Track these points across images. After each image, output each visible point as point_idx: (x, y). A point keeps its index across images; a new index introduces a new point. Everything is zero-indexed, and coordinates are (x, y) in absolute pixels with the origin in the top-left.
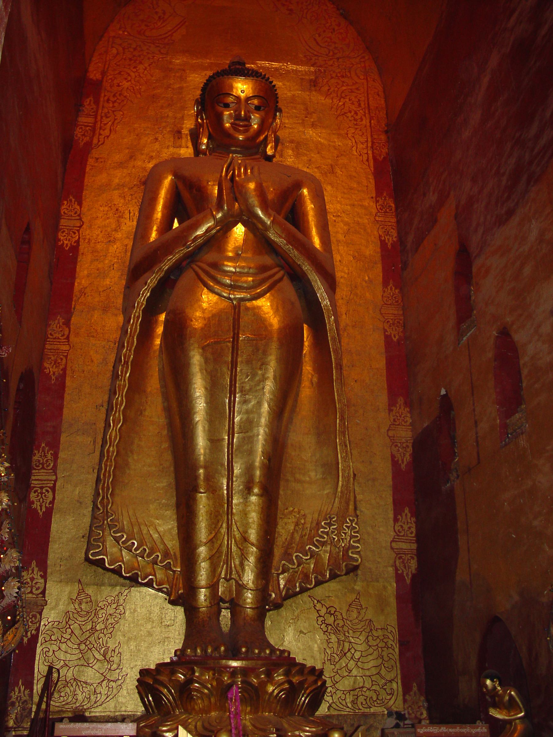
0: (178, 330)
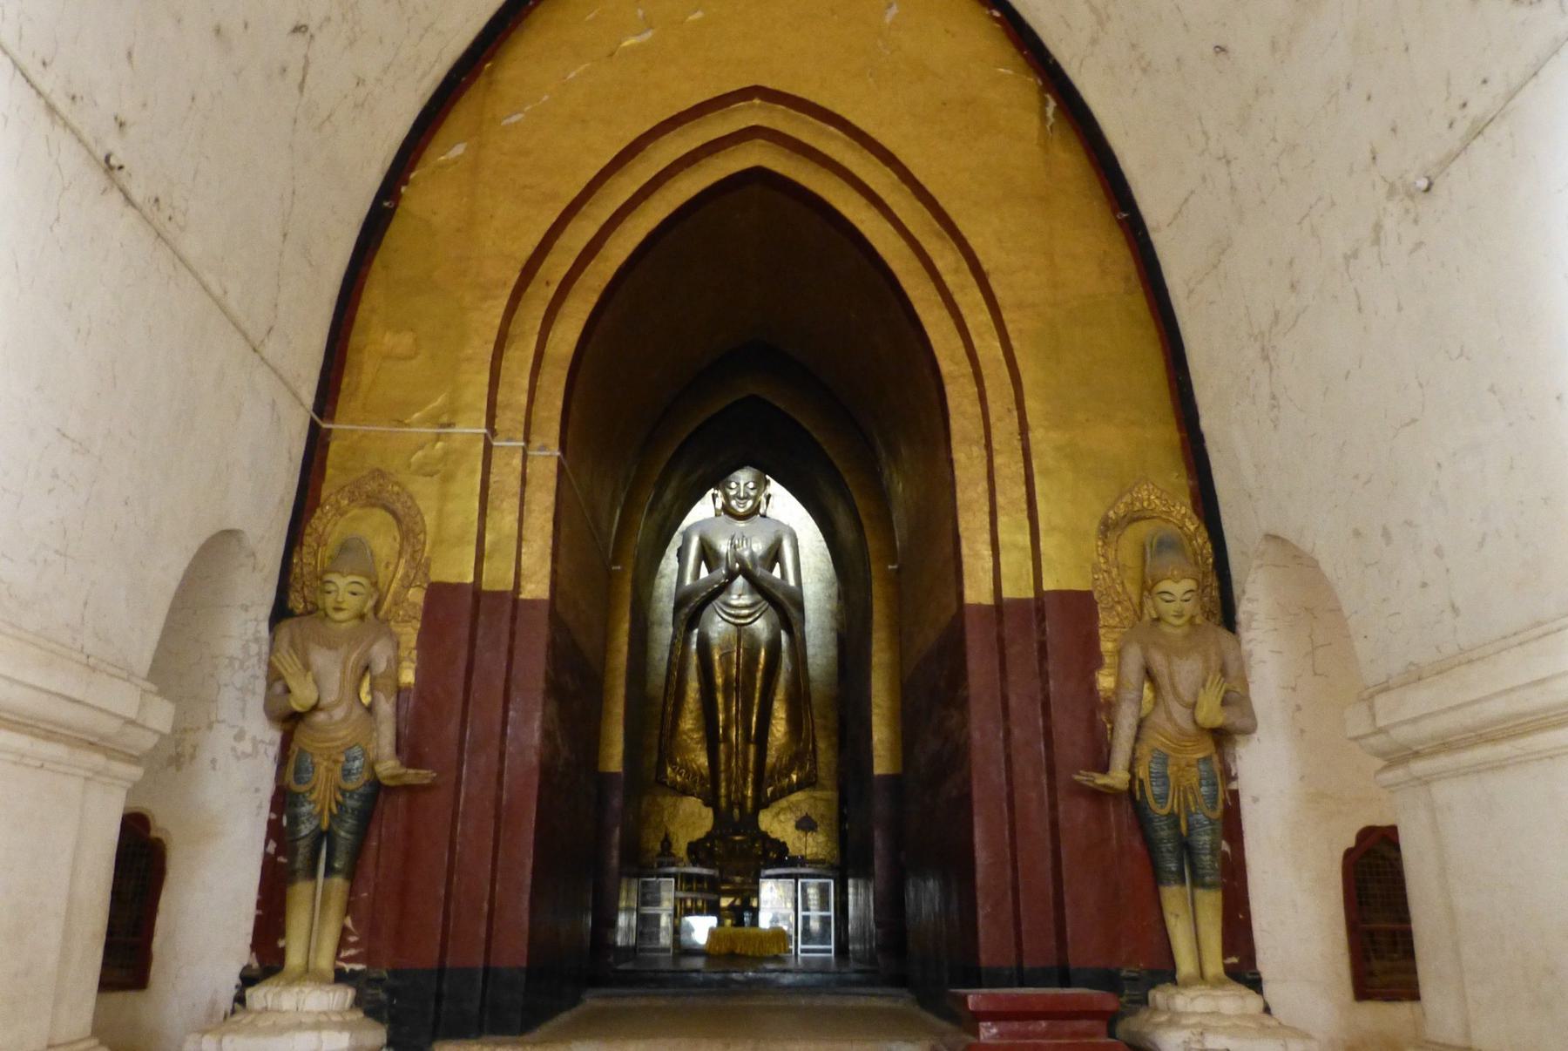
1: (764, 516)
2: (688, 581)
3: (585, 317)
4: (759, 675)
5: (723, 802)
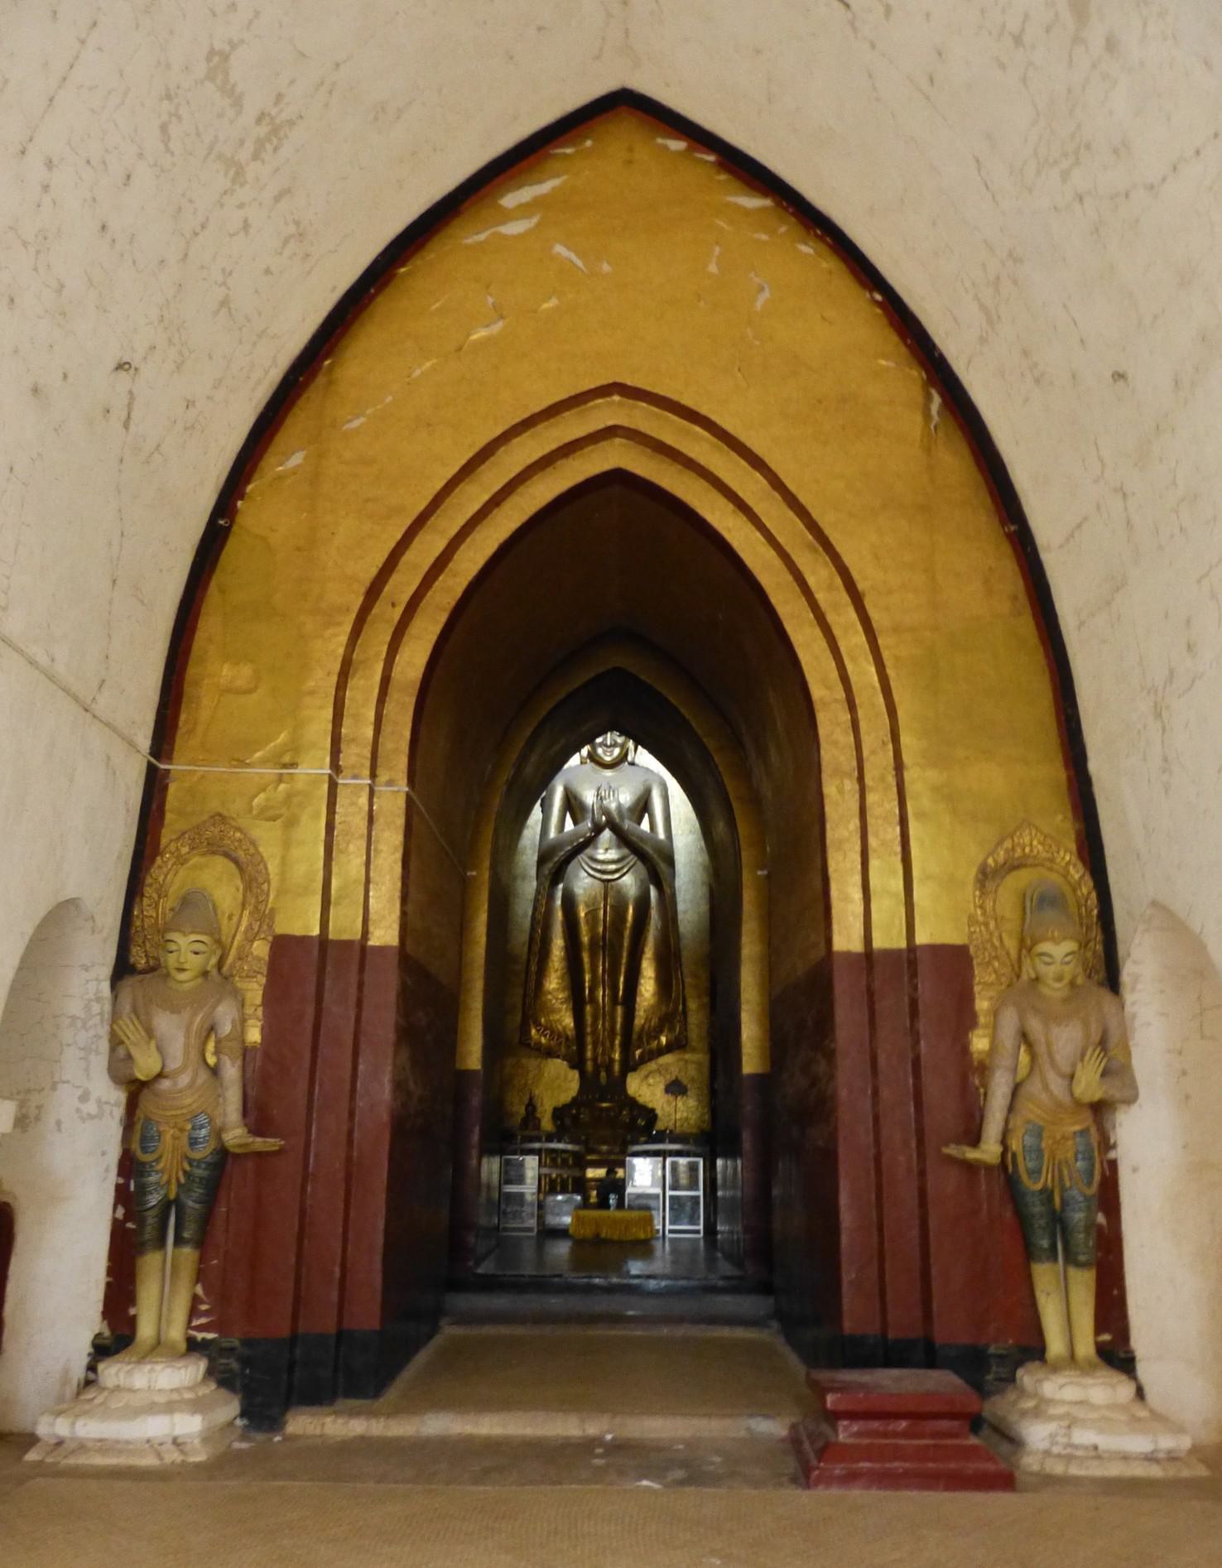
0: (569, 902)
1: (632, 764)
2: (552, 834)
3: (433, 638)
4: (627, 933)
5: (589, 1066)
